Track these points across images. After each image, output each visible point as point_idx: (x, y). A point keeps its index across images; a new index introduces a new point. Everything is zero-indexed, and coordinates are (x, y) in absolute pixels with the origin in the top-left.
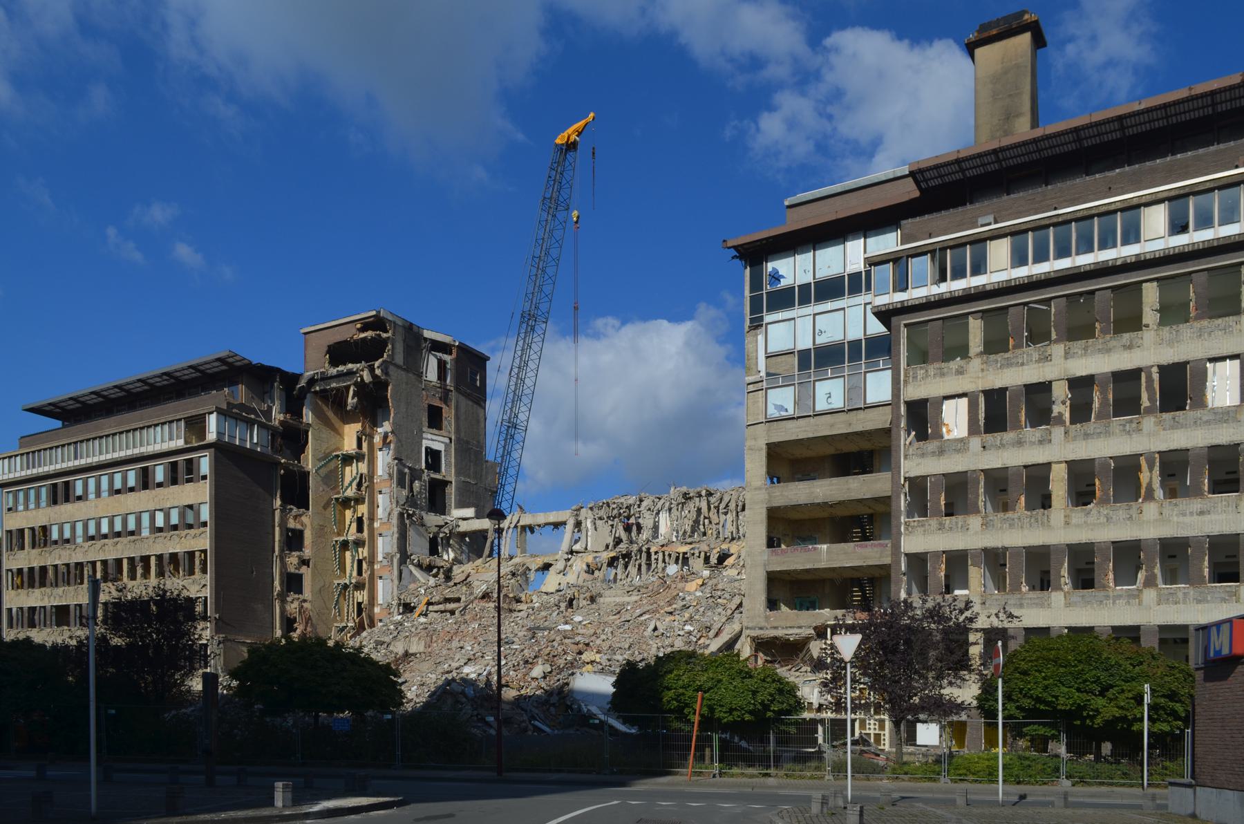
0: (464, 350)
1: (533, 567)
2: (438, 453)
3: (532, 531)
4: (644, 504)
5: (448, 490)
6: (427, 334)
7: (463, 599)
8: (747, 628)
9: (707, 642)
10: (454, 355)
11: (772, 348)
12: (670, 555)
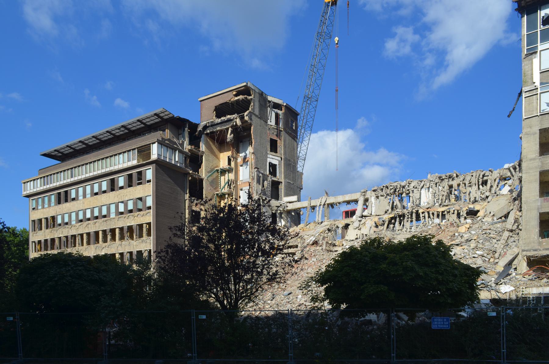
0: (288, 108)
1: (341, 226)
2: (276, 165)
3: (333, 207)
4: (412, 185)
5: (280, 187)
6: (270, 98)
7: (299, 245)
8: (523, 251)
9: (496, 261)
10: (283, 111)
11: (544, 67)
12: (433, 214)
